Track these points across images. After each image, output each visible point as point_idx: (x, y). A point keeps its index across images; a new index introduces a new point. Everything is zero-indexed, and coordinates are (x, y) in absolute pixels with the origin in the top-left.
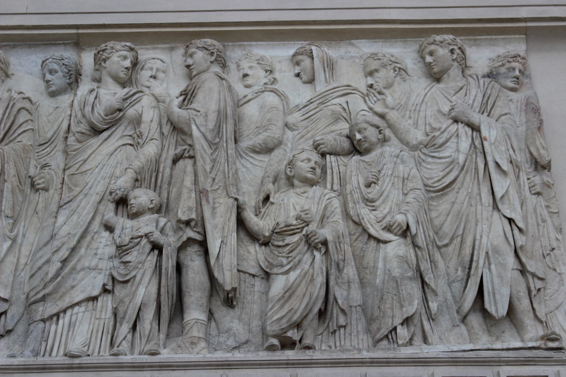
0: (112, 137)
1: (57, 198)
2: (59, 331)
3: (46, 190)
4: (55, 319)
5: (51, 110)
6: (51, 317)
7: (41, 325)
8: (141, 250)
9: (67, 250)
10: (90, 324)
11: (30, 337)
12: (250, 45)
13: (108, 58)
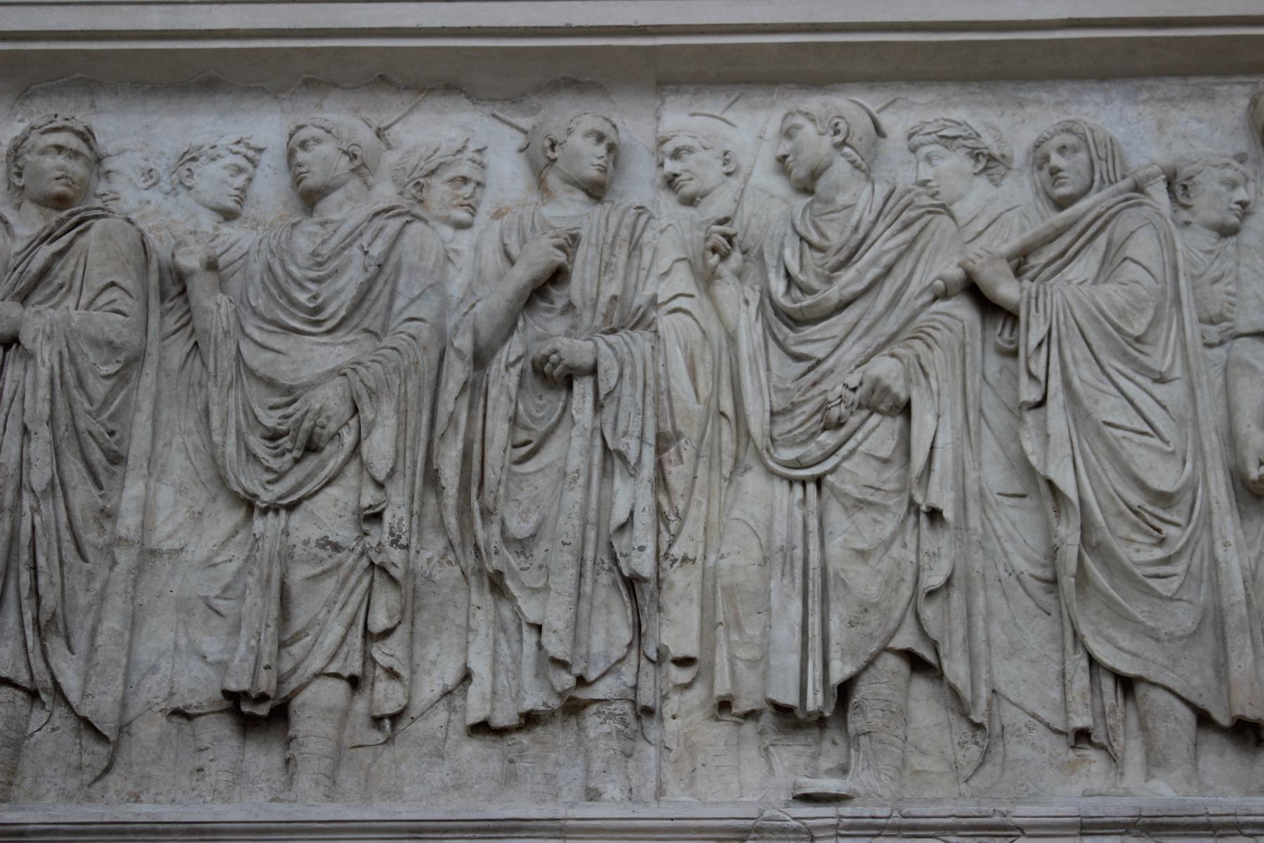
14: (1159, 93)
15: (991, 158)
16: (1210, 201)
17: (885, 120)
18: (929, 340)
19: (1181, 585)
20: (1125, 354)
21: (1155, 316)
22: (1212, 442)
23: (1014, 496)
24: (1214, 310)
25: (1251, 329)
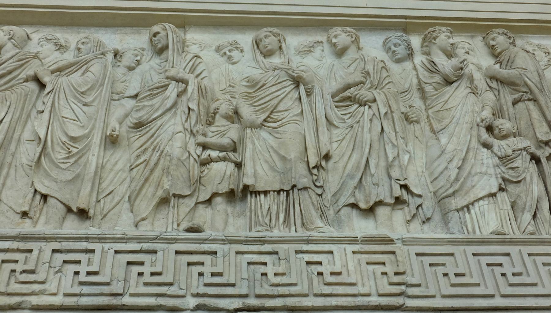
0: (460, 87)
1: (427, 128)
2: (474, 217)
3: (418, 122)
4: (465, 209)
5: (400, 71)
6: (462, 209)
7: (456, 213)
8: (524, 159)
9: (459, 160)
10: (496, 213)
11: (452, 222)
12: (528, 37)
13: (438, 37)
14: (123, 31)
15: (61, 46)
16: (127, 60)
17: (32, 36)
18: (12, 91)
19: (70, 166)
20: (75, 96)
21: (91, 87)
22: (100, 125)
23: (30, 141)
24: (119, 90)
25: (129, 96)
